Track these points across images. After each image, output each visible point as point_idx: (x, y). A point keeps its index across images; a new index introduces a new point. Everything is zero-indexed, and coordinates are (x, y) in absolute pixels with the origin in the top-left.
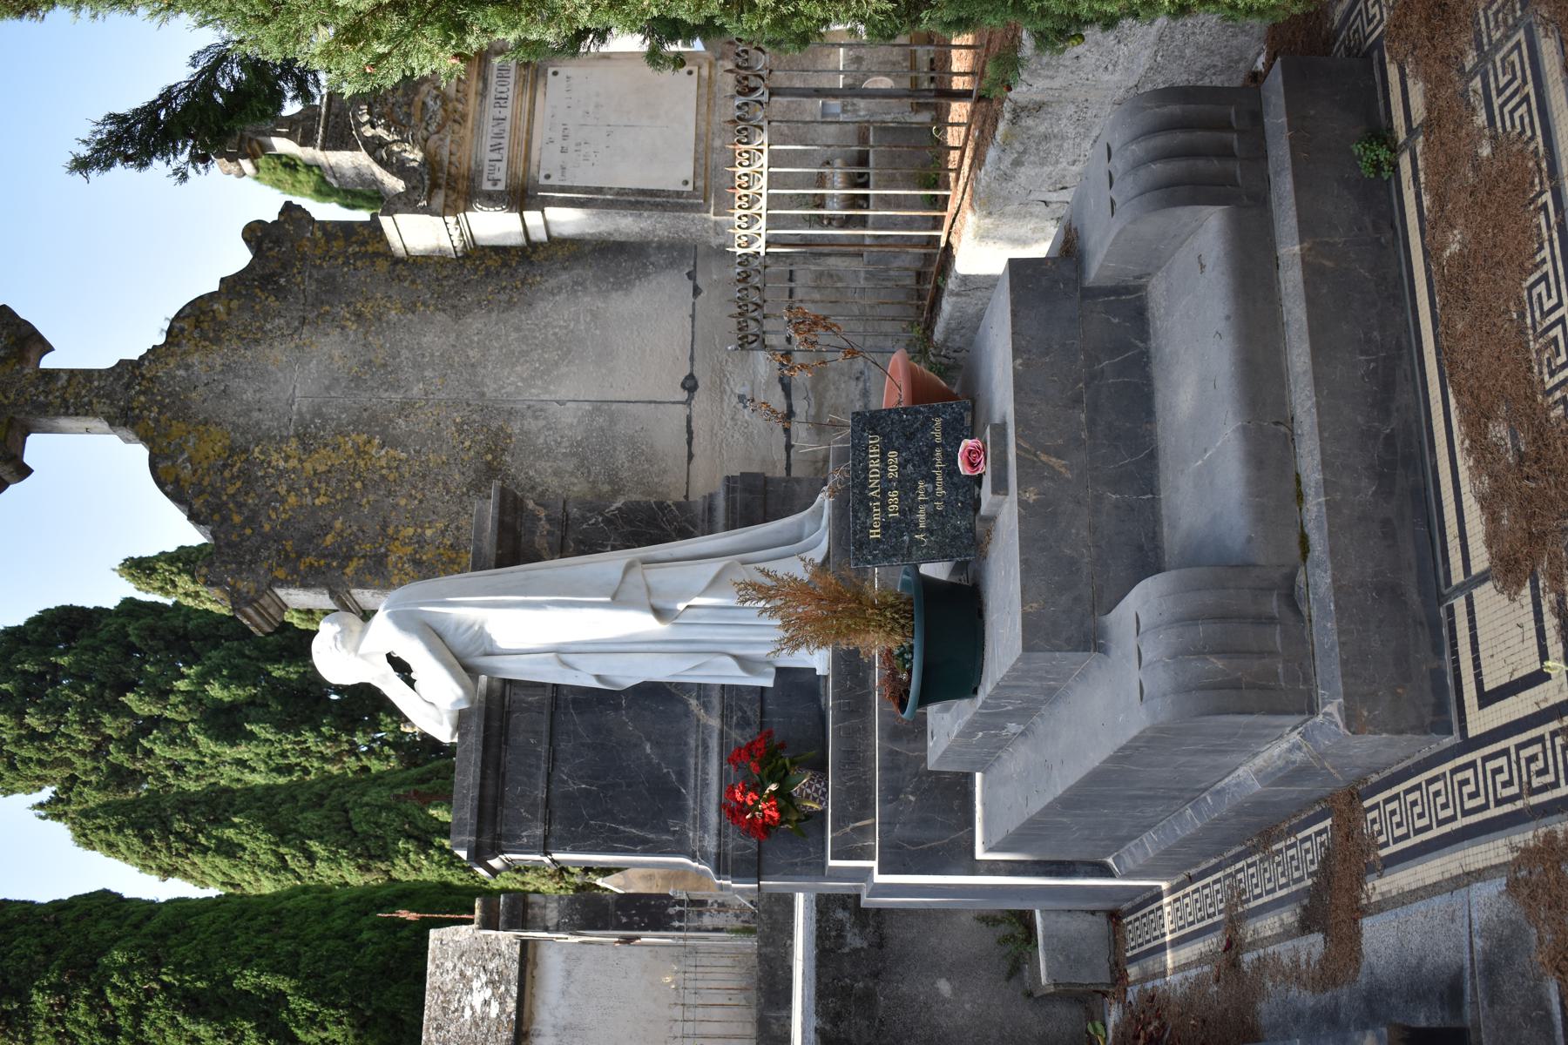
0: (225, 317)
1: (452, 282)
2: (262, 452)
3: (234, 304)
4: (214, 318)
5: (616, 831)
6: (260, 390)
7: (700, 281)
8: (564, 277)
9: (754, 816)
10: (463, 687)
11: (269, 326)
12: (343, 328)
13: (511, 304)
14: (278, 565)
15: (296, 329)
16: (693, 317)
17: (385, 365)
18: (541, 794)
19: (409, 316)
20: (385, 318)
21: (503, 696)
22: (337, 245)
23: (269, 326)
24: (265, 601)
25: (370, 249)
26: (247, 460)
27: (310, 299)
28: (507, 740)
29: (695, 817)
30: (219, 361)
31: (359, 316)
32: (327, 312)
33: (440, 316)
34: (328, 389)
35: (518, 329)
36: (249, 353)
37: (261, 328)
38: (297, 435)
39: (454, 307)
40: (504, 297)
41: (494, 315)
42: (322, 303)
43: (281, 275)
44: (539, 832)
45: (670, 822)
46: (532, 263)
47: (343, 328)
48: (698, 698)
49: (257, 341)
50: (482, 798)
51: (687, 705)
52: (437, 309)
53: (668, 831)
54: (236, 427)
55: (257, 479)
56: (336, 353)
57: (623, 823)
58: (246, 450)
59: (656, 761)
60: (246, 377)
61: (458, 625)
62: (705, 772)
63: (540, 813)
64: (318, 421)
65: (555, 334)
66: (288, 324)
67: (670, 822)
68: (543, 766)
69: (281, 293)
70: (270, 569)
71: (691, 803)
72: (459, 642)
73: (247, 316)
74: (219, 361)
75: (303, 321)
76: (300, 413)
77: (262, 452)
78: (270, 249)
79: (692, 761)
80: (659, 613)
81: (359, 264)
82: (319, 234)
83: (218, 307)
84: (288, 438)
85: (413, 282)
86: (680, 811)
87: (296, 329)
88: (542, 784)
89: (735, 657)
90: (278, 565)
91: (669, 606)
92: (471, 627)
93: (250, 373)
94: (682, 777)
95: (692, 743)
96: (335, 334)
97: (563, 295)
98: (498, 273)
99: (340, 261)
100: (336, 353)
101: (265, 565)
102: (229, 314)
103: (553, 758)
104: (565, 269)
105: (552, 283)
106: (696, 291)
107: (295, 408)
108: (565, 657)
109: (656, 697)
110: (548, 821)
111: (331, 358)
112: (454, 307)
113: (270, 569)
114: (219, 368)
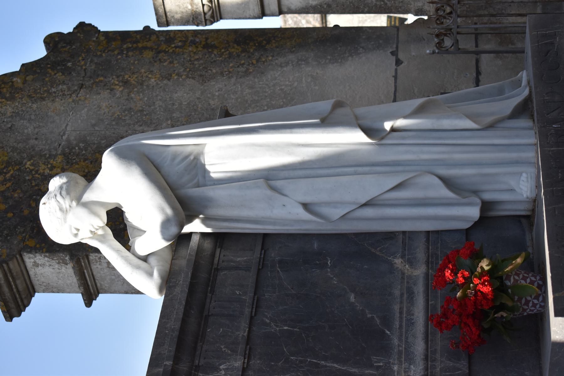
0: (21, 85)
1: (201, 62)
2: (32, 165)
3: (29, 78)
4: (12, 85)
5: (317, 365)
6: (39, 127)
7: (401, 56)
8: (291, 57)
9: (465, 296)
10: (173, 208)
11: (53, 90)
12: (112, 90)
13: (247, 73)
14: (31, 237)
15: (75, 91)
16: (396, 77)
17: (142, 111)
18: (243, 333)
19: (165, 82)
20: (146, 84)
21: (213, 255)
22: (114, 45)
23: (53, 90)
24: (13, 265)
25: (140, 45)
26: (19, 170)
27: (88, 74)
28: (212, 292)
29: (400, 353)
30: (10, 110)
31: (126, 83)
32: (101, 81)
33: (190, 82)
34: (93, 126)
35: (252, 87)
36: (35, 106)
37: (48, 91)
38: (63, 154)
39: (201, 76)
40: (242, 69)
41: (233, 80)
42: (98, 76)
43: (69, 61)
44: (238, 364)
45: (374, 358)
46: (266, 50)
47: (112, 90)
48: (403, 257)
49: (43, 99)
50: (182, 330)
51: (391, 264)
52: (187, 77)
53: (371, 366)
54: (14, 149)
55: (25, 181)
56: (104, 105)
57: (325, 359)
58: (20, 163)
59: (359, 307)
60: (30, 120)
61: (175, 156)
62: (410, 313)
63: (241, 347)
64: (82, 145)
65: (282, 90)
66: (69, 89)
67: (374, 358)
68: (247, 311)
69: (67, 71)
70: (23, 240)
71: (396, 341)
72: (174, 171)
73: (38, 85)
74: (10, 110)
75: (81, 86)
76: (68, 140)
77: (32, 165)
78: (63, 47)
79: (396, 308)
80: (368, 132)
81: (130, 54)
82: (102, 38)
83: (18, 80)
84: (56, 156)
85: (171, 62)
86: (384, 348)
87: (75, 91)
88: (244, 325)
89: (441, 178)
90: (31, 237)
91: (376, 125)
92: (187, 157)
93: (33, 117)
94: (387, 321)
95: (397, 292)
96: (106, 94)
97: (290, 67)
98: (238, 56)
99: (116, 52)
100: (104, 105)
101: (20, 238)
102: (24, 83)
103: (257, 304)
104: (292, 52)
105: (281, 60)
106: (398, 62)
107: (64, 138)
108: (273, 183)
109: (359, 251)
110: (248, 355)
111: (100, 107)
112: (201, 76)
113: (23, 240)
114: (9, 114)
